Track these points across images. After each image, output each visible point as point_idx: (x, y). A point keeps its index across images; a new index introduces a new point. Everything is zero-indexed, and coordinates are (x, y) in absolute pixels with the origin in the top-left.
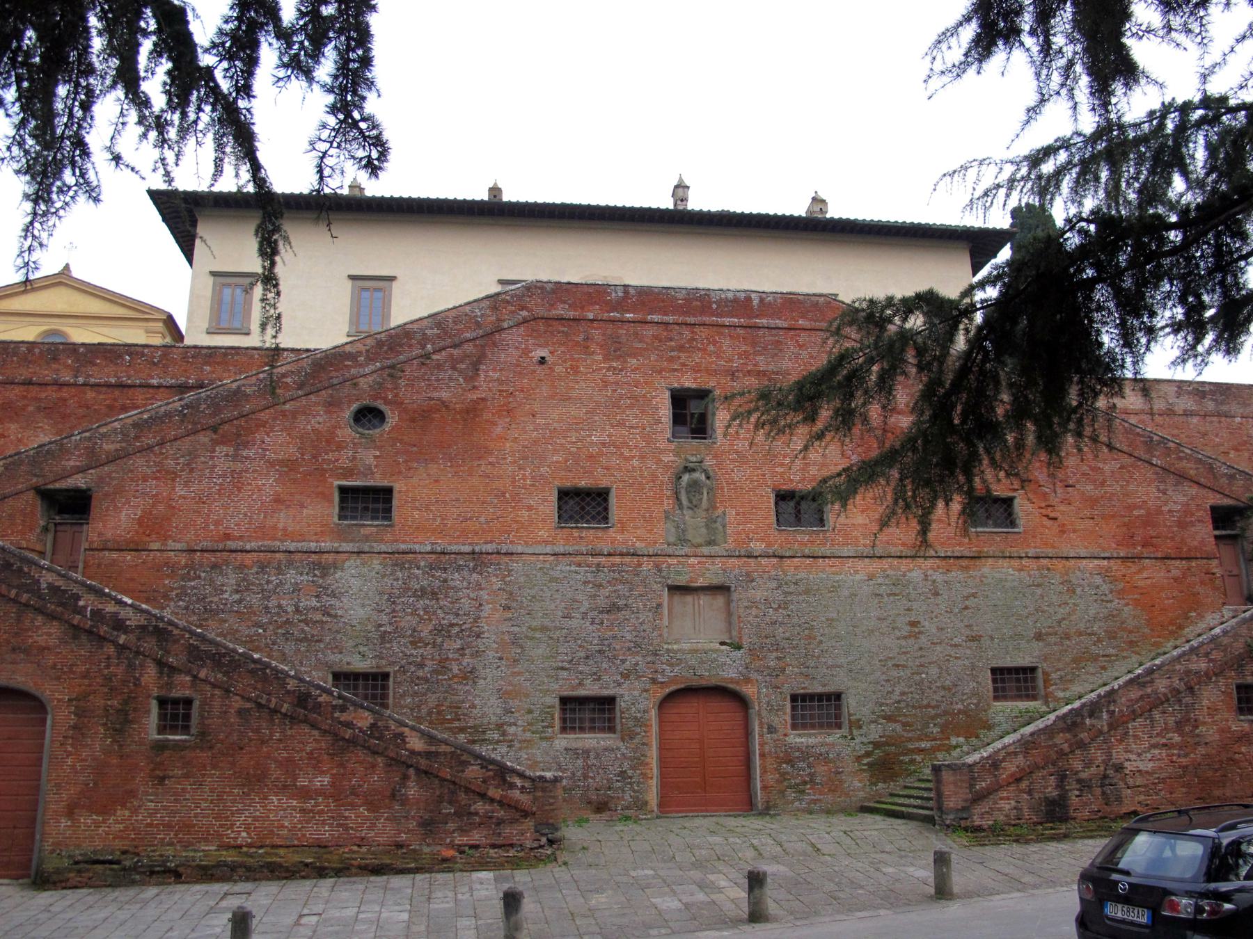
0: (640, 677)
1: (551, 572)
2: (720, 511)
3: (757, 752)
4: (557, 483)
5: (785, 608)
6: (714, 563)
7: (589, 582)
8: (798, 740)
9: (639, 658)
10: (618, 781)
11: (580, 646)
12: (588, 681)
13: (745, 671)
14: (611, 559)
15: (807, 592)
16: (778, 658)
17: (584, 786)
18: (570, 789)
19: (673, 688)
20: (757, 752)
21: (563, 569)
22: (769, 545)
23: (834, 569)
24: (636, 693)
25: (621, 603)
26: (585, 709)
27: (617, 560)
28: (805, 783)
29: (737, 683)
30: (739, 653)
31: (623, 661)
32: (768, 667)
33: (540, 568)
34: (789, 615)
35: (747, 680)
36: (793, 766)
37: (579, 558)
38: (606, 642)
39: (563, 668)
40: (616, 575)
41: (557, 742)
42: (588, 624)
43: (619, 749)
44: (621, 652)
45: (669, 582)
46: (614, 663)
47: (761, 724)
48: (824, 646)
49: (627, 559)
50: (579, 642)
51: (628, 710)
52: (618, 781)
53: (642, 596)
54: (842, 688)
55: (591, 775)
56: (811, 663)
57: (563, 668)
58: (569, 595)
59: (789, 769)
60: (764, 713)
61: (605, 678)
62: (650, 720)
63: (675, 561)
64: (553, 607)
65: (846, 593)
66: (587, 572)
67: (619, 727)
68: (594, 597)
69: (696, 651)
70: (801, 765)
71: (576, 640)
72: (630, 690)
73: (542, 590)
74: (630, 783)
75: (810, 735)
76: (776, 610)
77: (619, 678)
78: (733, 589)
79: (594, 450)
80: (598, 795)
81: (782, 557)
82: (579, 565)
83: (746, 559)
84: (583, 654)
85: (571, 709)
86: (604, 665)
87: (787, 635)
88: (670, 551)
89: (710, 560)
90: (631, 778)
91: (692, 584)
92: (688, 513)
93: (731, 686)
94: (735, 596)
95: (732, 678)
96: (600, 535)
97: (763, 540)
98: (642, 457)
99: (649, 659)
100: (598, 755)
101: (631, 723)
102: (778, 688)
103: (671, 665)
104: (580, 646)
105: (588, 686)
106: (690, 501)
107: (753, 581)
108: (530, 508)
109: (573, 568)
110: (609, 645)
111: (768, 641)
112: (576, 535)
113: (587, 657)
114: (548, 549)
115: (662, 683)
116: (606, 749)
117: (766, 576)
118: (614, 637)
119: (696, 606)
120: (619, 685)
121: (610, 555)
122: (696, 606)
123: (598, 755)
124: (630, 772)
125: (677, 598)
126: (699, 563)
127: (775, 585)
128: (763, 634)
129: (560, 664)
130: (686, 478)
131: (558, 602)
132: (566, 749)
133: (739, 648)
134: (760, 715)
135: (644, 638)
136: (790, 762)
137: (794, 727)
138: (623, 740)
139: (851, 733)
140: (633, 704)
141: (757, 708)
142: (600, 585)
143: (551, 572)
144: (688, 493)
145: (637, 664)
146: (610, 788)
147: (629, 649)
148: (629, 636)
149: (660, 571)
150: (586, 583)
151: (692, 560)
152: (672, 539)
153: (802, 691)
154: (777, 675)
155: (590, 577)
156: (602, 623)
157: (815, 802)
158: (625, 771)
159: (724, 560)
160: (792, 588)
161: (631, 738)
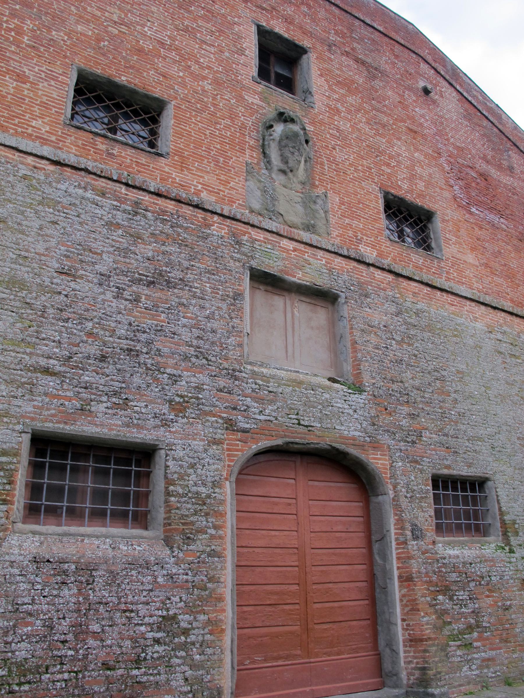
0: (206, 413)
1: (48, 190)
2: (320, 191)
3: (396, 573)
4: (80, 62)
5: (409, 345)
6: (314, 256)
7: (118, 226)
8: (451, 552)
9: (203, 378)
10: (157, 641)
11: (90, 334)
12: (102, 407)
13: (370, 429)
14: (160, 201)
15: (430, 328)
16: (412, 416)
17: (74, 659)
18: (37, 670)
19: (264, 443)
20: (396, 573)
21: (71, 190)
22: (380, 255)
23: (453, 308)
24: (198, 444)
25: (175, 274)
26: (85, 470)
27: (170, 205)
28: (470, 628)
29: (361, 446)
30: (358, 399)
31: (175, 379)
32: (401, 427)
33: (25, 177)
34: (416, 356)
35: (376, 445)
36: (451, 599)
37: (102, 183)
38: (143, 337)
39: (47, 371)
40: (167, 229)
41: (14, 540)
42: (109, 295)
43: (159, 563)
44: (171, 362)
45: (254, 264)
46: (156, 380)
47: (400, 521)
48: (461, 407)
49: (187, 211)
50: (90, 325)
51: (181, 478)
52: (157, 641)
53: (209, 272)
54: (489, 473)
55: (95, 627)
56: (450, 429)
57: (47, 371)
58: (79, 236)
59: (448, 605)
60: (404, 503)
61: (139, 405)
62: (222, 502)
63: (260, 236)
64: (40, 247)
65: (470, 342)
66: (116, 208)
67: (160, 514)
68: (126, 252)
69: (300, 383)
70: (462, 595)
71: (82, 319)
72: (186, 436)
73: (22, 213)
74: (184, 647)
75: (462, 545)
76: (398, 343)
77: (165, 409)
78: (342, 300)
79: (148, 46)
80: (109, 681)
81: (398, 275)
82: (103, 194)
83: (355, 264)
84: (93, 349)
85: (52, 467)
86: (137, 380)
87: (417, 383)
88: (255, 219)
89: (310, 250)
90: (186, 632)
91: (287, 277)
92: (280, 178)
93: (353, 451)
94: (345, 311)
95: (354, 438)
96: (143, 161)
97: (373, 247)
98: (217, 83)
99: (222, 383)
100: (113, 575)
101: (187, 508)
102: (416, 462)
103: (260, 400)
104: (90, 334)
105: (100, 418)
106: (285, 161)
107: (367, 296)
108: (21, 78)
109: (89, 194)
110: (149, 343)
111: (395, 387)
112: (103, 147)
113: (103, 358)
114: (46, 151)
115: (245, 431)
116: (132, 564)
117: (382, 294)
118: (159, 331)
119: (289, 315)
120: (166, 424)
121: (158, 195)
122: (289, 315)
123: (113, 575)
124: (184, 620)
125: (261, 296)
126: (295, 250)
127: (393, 309)
128: (389, 376)
129: (43, 362)
130: (279, 129)
131: (53, 242)
132: (35, 560)
133: (360, 390)
134: (397, 507)
135: (213, 343)
136: (445, 590)
137: (439, 529)
138: (168, 542)
139: (508, 543)
140: (192, 466)
141: (391, 494)
142: (137, 237)
143: (48, 190)
144: (281, 147)
145: (199, 388)
146: (138, 662)
147: (186, 358)
148: (186, 335)
149: (239, 243)
150: (111, 225)
151: (285, 243)
152: (256, 206)
153: (445, 472)
154: (414, 442)
155: (120, 217)
156: (137, 300)
157: (487, 662)
158: (174, 618)
159: (328, 255)
160: (413, 320)
161: (188, 540)
